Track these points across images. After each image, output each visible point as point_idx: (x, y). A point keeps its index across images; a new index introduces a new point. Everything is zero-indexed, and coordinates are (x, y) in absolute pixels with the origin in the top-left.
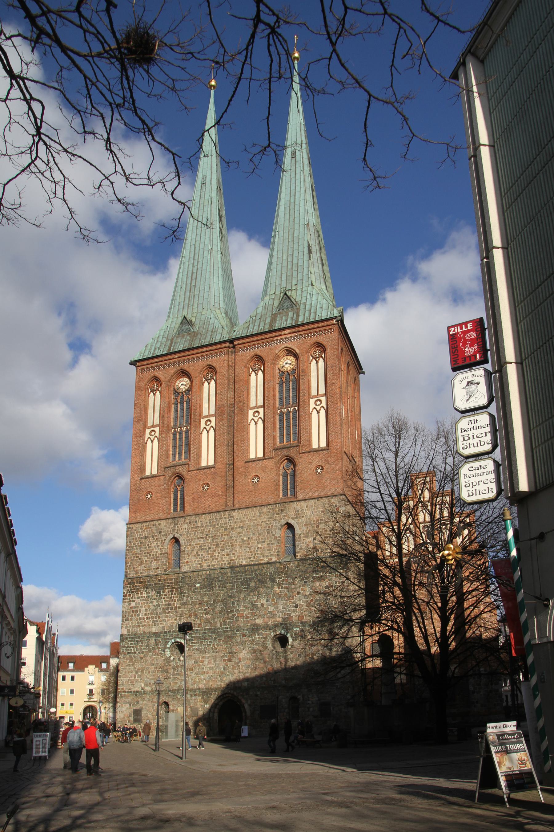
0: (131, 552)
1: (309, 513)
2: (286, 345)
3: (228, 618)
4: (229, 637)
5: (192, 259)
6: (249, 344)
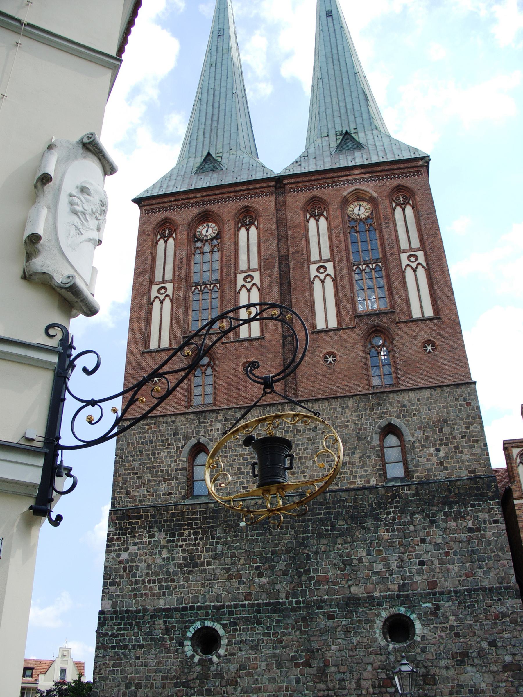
0: (125, 466)
1: (424, 409)
2: (357, 187)
4: (304, 620)
6: (305, 184)
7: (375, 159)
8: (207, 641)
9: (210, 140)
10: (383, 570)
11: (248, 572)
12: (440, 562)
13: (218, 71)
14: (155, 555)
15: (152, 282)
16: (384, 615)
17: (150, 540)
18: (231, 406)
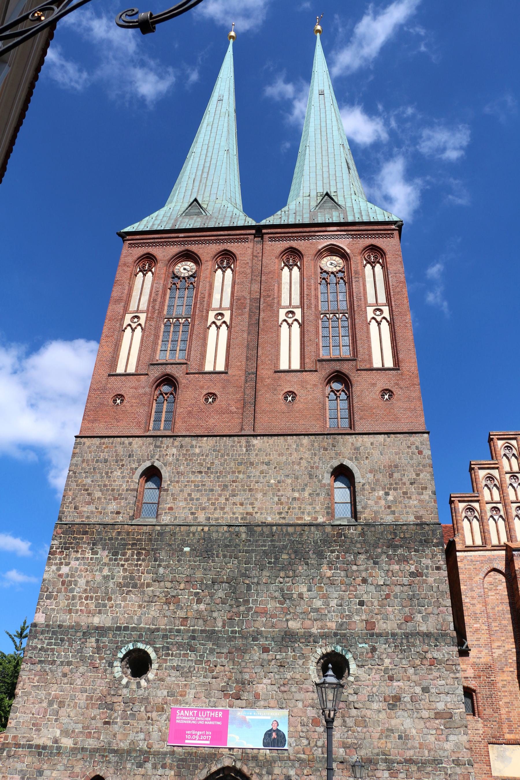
1: (376, 453)
3: (238, 614)
4: (238, 649)
5: (203, 157)
7: (350, 219)
8: (138, 664)
9: (199, 188)
10: (323, 607)
11: (186, 597)
12: (380, 603)
13: (214, 130)
14: (95, 572)
15: (126, 310)
16: (320, 652)
17: (92, 556)
18: (188, 434)
